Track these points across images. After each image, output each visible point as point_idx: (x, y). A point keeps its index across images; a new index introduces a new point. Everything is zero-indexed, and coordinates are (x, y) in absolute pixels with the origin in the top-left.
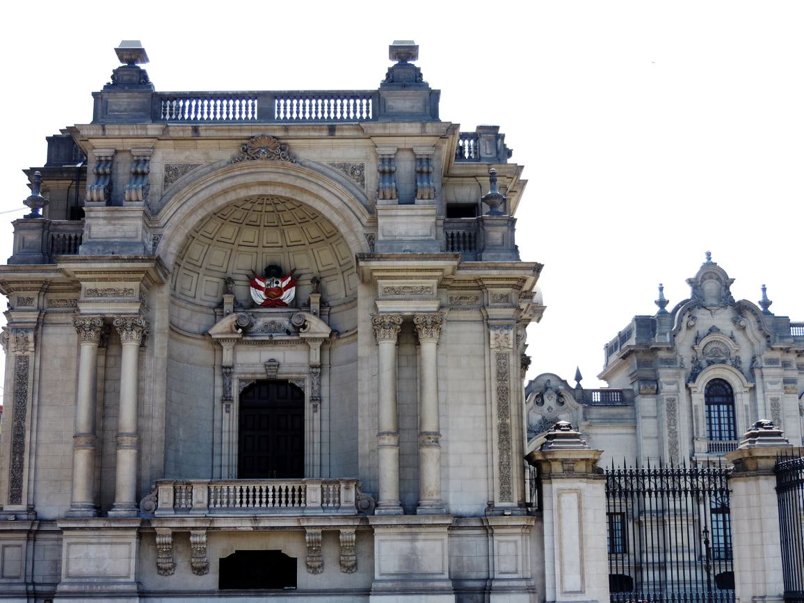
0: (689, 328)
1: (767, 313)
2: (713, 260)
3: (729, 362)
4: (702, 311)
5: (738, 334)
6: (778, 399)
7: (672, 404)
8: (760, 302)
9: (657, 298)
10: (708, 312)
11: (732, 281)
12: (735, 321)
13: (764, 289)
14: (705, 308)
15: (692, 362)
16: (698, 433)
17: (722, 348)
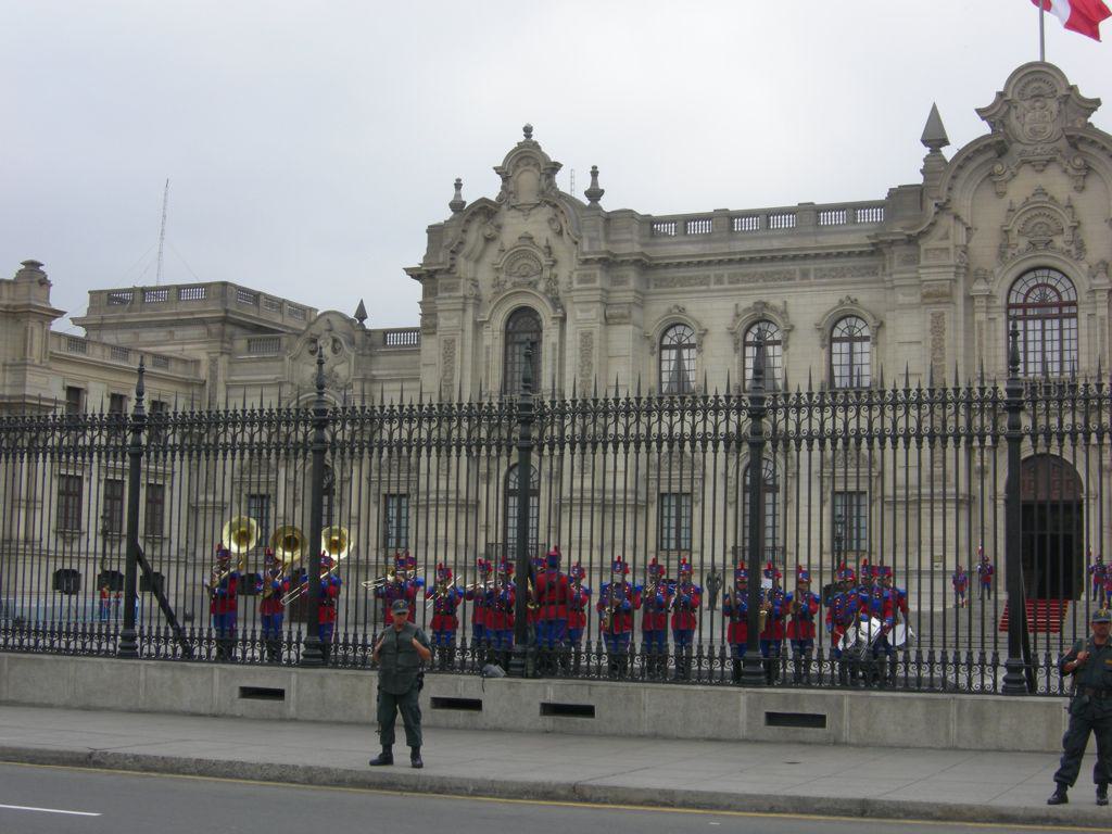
0: (488, 240)
1: (594, 207)
2: (533, 138)
3: (542, 286)
4: (513, 213)
5: (556, 243)
6: (591, 333)
7: (449, 347)
8: (588, 194)
9: (451, 198)
10: (521, 213)
11: (556, 167)
12: (551, 221)
13: (595, 173)
14: (513, 207)
15: (493, 287)
16: (487, 385)
17: (533, 264)
